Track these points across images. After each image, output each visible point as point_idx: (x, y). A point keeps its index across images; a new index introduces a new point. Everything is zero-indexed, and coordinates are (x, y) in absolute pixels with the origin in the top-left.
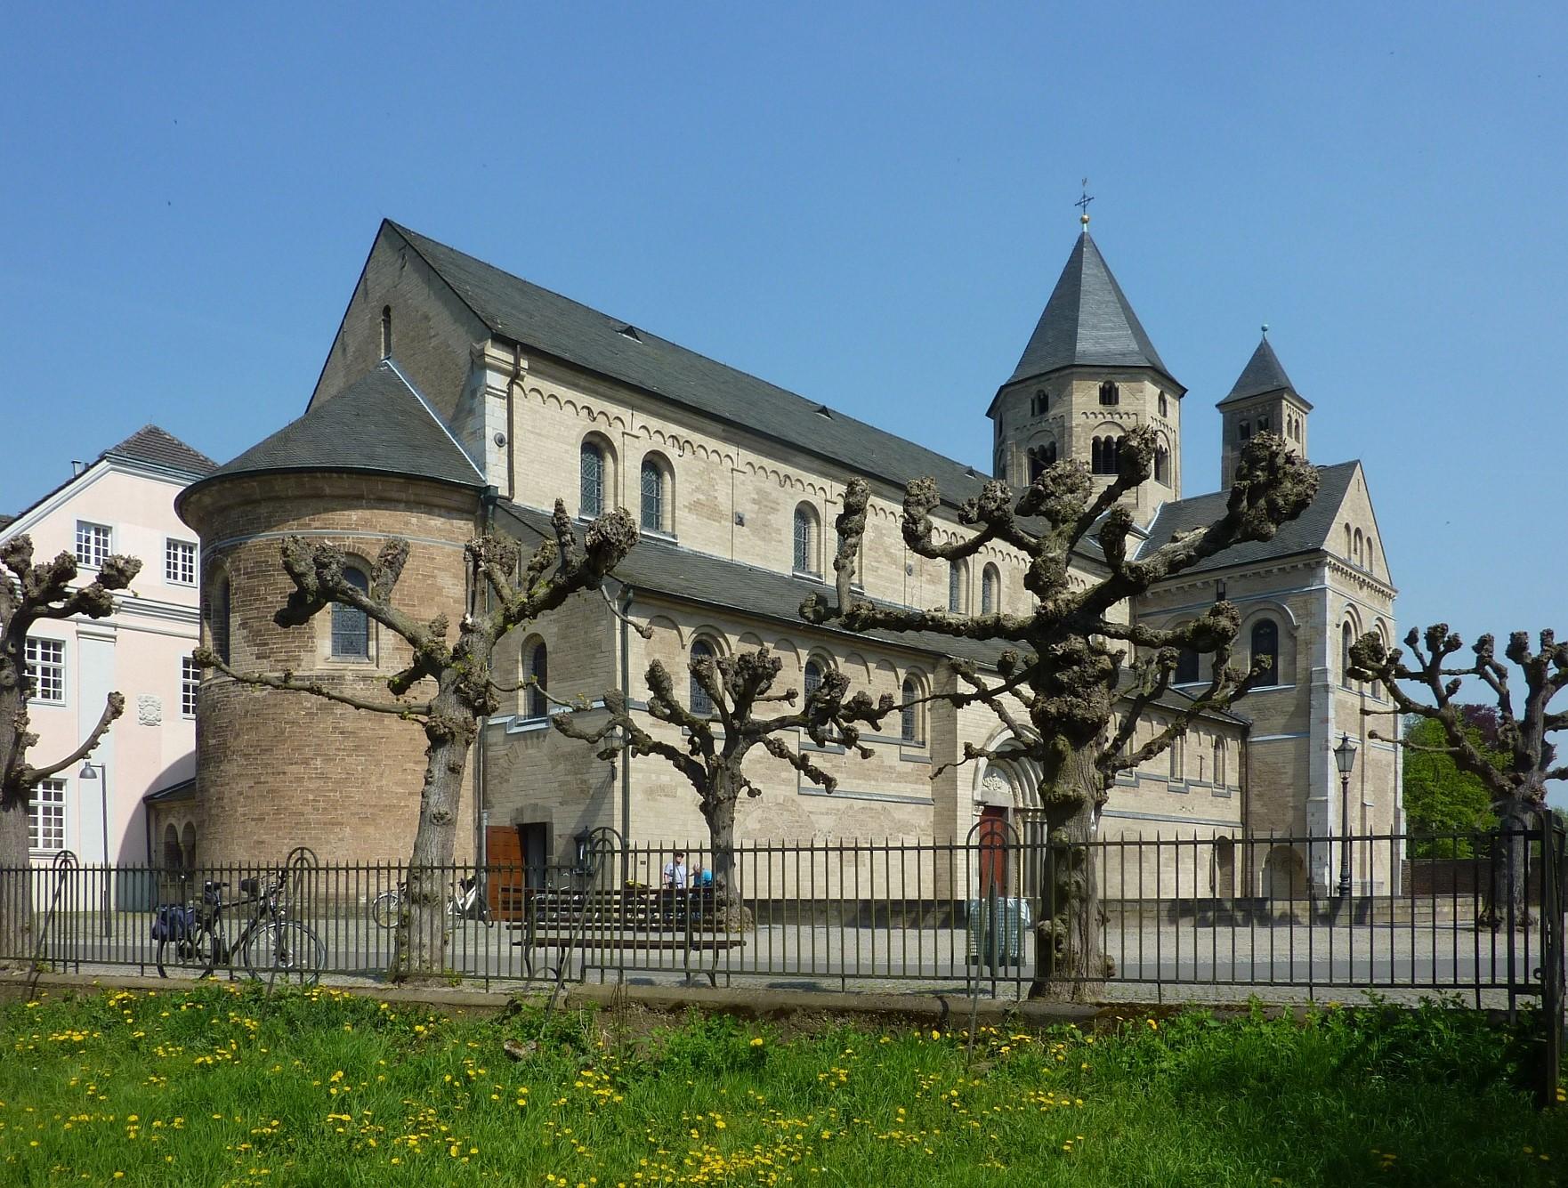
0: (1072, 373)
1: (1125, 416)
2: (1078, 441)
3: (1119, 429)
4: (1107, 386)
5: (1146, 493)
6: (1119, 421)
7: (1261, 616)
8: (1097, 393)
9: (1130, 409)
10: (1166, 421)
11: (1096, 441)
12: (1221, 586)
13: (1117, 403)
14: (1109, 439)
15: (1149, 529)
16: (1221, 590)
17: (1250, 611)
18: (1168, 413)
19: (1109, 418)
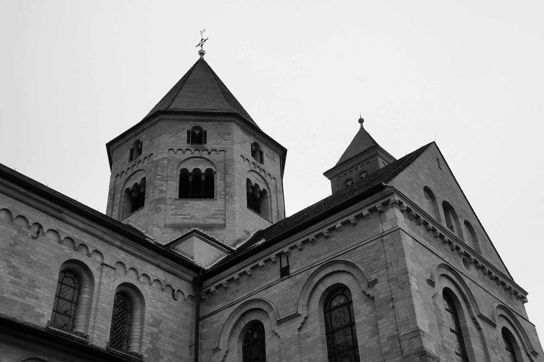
0: (160, 120)
1: (213, 153)
2: (163, 171)
3: (208, 163)
4: (197, 132)
5: (234, 214)
6: (207, 156)
7: (330, 282)
8: (184, 135)
9: (218, 147)
10: (262, 166)
11: (184, 174)
12: (284, 260)
13: (205, 142)
14: (197, 171)
15: (237, 247)
16: (284, 265)
17: (316, 280)
18: (265, 162)
19: (197, 154)
